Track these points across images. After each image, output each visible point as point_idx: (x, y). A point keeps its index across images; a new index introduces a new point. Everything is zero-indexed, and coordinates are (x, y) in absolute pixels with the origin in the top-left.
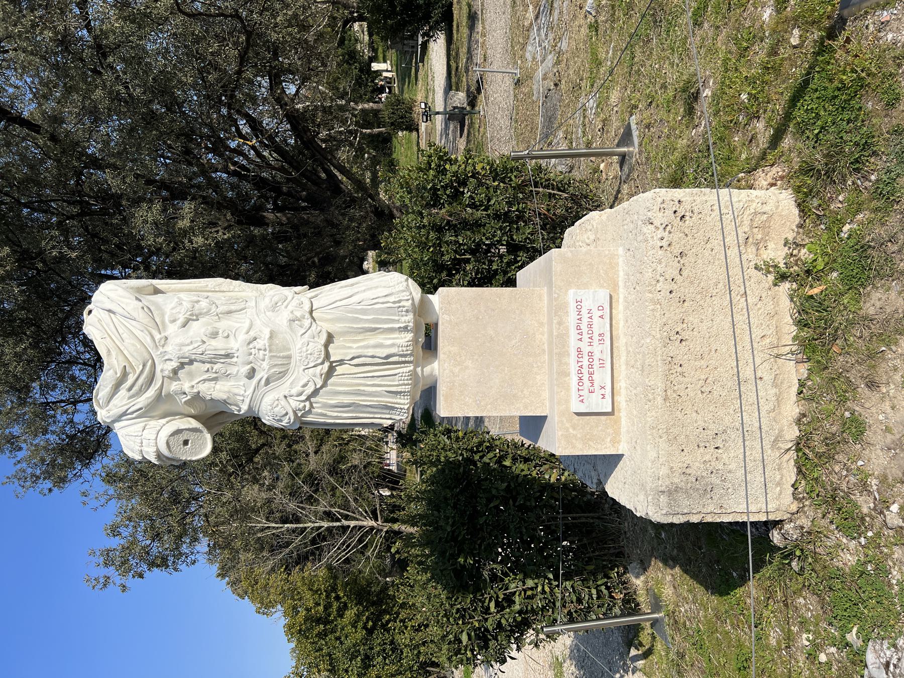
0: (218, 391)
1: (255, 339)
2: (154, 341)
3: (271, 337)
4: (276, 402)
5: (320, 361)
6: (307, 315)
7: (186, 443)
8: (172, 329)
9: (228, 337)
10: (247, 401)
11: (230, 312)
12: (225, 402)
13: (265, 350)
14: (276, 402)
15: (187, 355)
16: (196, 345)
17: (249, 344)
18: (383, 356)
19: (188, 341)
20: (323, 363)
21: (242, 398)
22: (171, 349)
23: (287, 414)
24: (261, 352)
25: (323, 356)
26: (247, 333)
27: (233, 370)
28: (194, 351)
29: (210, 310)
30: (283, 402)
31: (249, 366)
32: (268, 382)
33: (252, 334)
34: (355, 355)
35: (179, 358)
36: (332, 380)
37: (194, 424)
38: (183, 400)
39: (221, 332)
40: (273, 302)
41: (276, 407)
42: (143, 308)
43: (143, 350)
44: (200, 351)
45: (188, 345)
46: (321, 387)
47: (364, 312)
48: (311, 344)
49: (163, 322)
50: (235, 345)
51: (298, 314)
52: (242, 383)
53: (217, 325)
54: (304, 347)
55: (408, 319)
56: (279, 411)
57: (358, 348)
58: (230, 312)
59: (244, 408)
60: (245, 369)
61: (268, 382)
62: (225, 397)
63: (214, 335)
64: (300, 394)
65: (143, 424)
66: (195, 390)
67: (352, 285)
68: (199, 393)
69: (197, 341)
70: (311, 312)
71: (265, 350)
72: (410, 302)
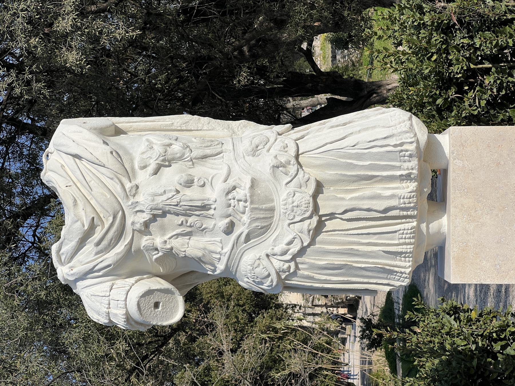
0: (193, 247)
1: (234, 188)
2: (125, 190)
3: (252, 187)
4: (258, 262)
5: (308, 214)
6: (293, 161)
7: (156, 305)
8: (143, 177)
9: (203, 185)
10: (224, 260)
11: (205, 157)
12: (199, 260)
13: (246, 201)
14: (258, 262)
15: (161, 206)
16: (170, 195)
17: (228, 194)
18: (382, 208)
19: (162, 191)
20: (310, 217)
21: (218, 256)
22: (143, 198)
23: (269, 275)
24: (241, 203)
25: (311, 209)
26: (225, 181)
27: (209, 224)
28: (168, 202)
29: (183, 155)
30: (265, 262)
31: (227, 220)
32: (248, 239)
33: (231, 182)
34: (348, 208)
35: (151, 209)
36: (321, 237)
37: (165, 285)
38: (155, 257)
39: (196, 180)
40: (254, 146)
41: (255, 266)
42: (111, 153)
43: (114, 200)
44: (174, 201)
45: (161, 195)
46: (309, 245)
47: (359, 157)
48: (297, 194)
49: (133, 169)
50: (213, 194)
51: (283, 159)
52: (218, 239)
53: (192, 172)
54: (289, 197)
55: (412, 165)
56: (260, 271)
57: (351, 199)
58: (205, 157)
59: (221, 267)
60: (223, 223)
61: (248, 239)
62: (199, 254)
63: (189, 183)
64: (284, 253)
65: (109, 284)
66: (168, 246)
67: (345, 124)
68: (172, 249)
69: (170, 191)
70: (297, 157)
71: (246, 201)
72: (415, 145)
